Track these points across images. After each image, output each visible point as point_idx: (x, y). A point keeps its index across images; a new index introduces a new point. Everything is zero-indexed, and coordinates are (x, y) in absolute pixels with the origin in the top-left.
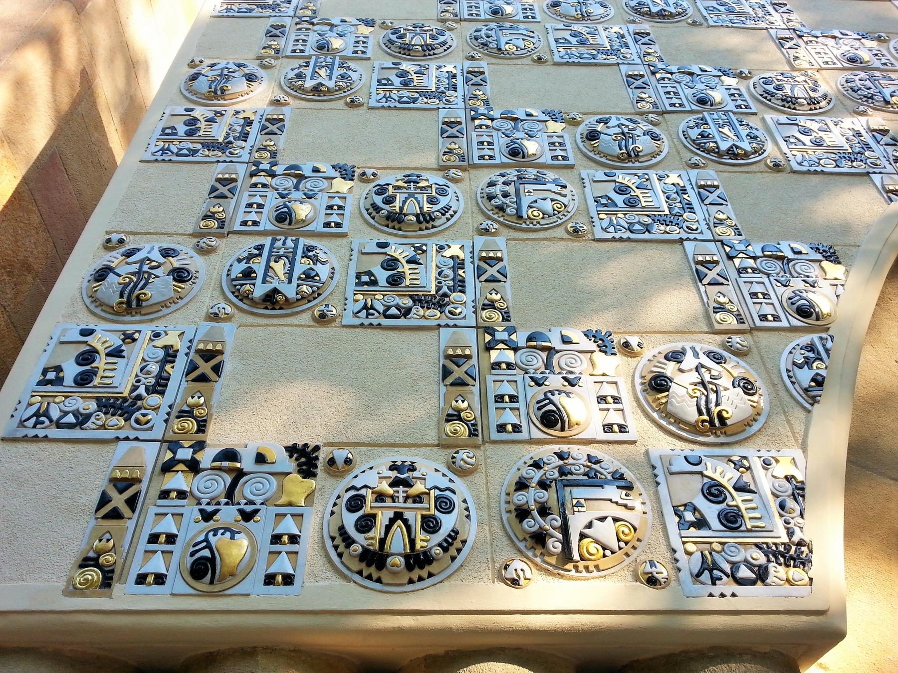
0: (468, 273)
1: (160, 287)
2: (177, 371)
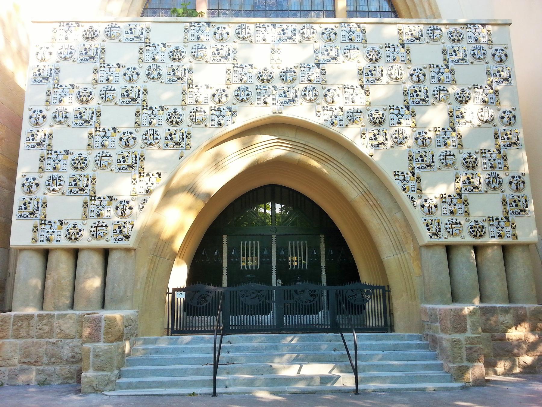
0: (185, 137)
1: (131, 142)
2: (138, 159)
